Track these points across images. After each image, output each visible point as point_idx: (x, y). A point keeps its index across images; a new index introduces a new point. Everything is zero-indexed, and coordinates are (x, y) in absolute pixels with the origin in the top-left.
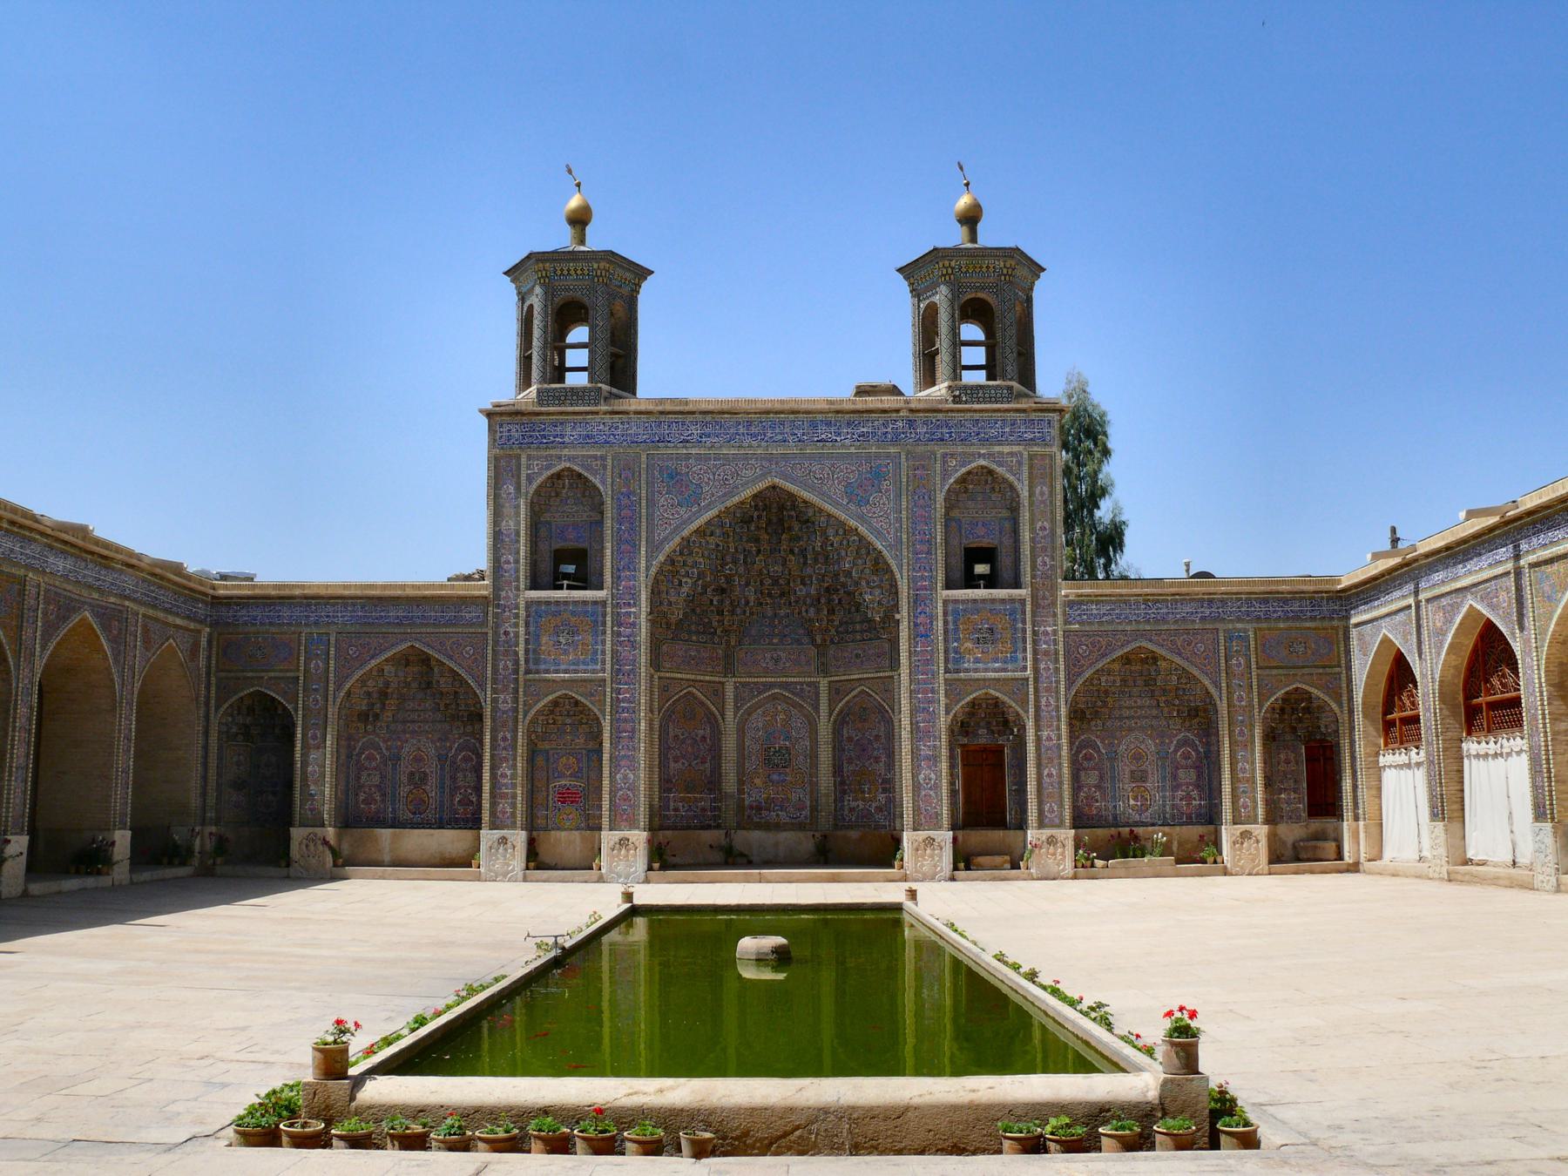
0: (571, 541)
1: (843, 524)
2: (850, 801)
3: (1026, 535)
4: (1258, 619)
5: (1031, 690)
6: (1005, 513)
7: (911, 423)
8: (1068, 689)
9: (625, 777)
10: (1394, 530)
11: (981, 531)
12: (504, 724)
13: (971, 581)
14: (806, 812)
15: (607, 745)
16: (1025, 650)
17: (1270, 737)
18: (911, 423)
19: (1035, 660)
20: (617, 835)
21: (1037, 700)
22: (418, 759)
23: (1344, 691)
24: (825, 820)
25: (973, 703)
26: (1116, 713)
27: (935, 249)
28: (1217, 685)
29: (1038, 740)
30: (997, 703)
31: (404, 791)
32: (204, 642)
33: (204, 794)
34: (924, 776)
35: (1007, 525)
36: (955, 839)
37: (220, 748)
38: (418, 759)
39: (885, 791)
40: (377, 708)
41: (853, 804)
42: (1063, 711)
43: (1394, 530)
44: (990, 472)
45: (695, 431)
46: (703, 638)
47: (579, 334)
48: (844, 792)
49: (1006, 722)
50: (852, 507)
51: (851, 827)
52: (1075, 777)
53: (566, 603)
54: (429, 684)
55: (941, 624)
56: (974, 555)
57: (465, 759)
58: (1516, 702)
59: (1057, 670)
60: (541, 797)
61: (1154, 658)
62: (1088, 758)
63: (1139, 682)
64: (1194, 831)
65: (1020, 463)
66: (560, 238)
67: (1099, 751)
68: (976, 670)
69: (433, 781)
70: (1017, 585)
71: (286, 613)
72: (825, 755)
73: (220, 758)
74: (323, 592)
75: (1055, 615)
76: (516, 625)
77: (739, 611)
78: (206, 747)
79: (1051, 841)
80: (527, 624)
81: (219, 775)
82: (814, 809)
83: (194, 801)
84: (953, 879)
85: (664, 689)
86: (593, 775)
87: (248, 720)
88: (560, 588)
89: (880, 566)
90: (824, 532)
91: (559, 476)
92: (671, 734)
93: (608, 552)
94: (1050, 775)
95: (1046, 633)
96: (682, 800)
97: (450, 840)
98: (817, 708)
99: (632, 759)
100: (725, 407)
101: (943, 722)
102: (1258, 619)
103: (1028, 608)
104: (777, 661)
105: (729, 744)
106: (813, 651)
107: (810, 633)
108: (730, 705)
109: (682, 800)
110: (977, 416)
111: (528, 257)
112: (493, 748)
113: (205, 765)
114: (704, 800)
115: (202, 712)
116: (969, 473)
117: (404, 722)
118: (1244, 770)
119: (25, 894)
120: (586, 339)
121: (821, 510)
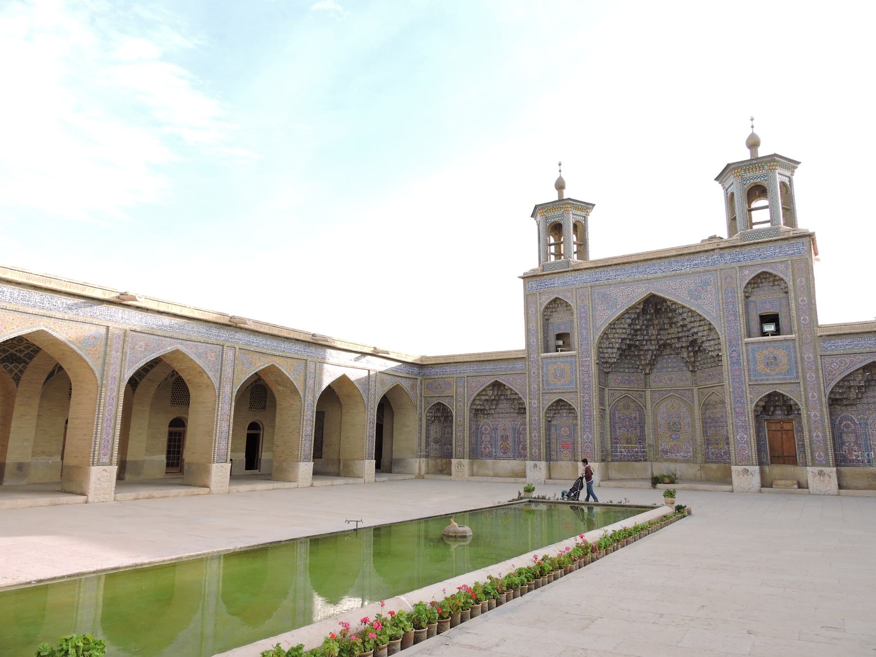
1: (691, 311)
3: (793, 305)
5: (802, 389)
6: (783, 295)
9: (588, 437)
12: (534, 413)
16: (797, 367)
18: (721, 255)
22: (505, 430)
25: (769, 395)
27: (728, 165)
29: (809, 416)
30: (783, 396)
31: (499, 443)
32: (419, 383)
34: (742, 434)
37: (427, 426)
38: (505, 430)
40: (487, 408)
41: (713, 450)
42: (825, 400)
45: (612, 274)
46: (632, 370)
48: (709, 444)
49: (791, 406)
50: (692, 301)
51: (712, 462)
53: (559, 357)
55: (745, 356)
59: (818, 377)
60: (553, 446)
62: (848, 426)
65: (787, 268)
66: (554, 196)
67: (854, 423)
68: (767, 380)
72: (698, 425)
73: (428, 431)
76: (538, 369)
77: (648, 357)
79: (821, 473)
81: (427, 437)
82: (695, 452)
83: (416, 446)
84: (760, 491)
87: (439, 414)
92: (617, 416)
93: (576, 334)
94: (817, 436)
95: (809, 358)
96: (624, 448)
98: (693, 402)
100: (625, 261)
101: (750, 407)
103: (797, 345)
105: (649, 420)
106: (689, 374)
109: (624, 448)
110: (758, 246)
111: (536, 208)
114: (637, 448)
116: (758, 276)
117: (499, 413)
119: (312, 486)
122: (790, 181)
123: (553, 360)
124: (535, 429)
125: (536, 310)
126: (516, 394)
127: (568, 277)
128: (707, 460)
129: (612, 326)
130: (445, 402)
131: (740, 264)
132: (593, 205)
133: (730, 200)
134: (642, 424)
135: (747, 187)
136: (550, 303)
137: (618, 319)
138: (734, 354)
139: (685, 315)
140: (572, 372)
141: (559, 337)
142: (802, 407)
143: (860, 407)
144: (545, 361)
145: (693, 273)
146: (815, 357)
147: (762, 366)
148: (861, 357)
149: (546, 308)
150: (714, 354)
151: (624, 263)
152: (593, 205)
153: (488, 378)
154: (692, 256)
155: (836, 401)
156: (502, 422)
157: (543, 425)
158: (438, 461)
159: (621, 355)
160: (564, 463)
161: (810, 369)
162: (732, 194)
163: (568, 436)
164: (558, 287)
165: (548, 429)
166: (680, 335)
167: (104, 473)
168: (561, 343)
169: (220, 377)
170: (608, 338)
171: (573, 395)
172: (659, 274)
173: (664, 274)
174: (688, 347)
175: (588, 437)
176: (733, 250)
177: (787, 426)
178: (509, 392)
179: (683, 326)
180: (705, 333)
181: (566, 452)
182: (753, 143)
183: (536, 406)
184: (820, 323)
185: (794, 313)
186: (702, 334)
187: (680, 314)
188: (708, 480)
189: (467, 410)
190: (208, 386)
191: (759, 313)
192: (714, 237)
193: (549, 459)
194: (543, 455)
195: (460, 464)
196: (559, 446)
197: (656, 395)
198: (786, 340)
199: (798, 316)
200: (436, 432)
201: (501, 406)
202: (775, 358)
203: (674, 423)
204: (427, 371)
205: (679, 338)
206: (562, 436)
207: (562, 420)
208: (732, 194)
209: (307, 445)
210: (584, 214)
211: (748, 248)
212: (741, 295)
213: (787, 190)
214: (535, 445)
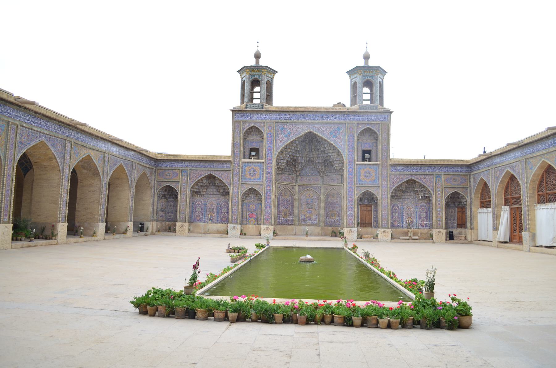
0: (254, 146)
1: (329, 143)
2: (329, 219)
3: (380, 147)
6: (375, 141)
7: (349, 115)
8: (390, 190)
9: (268, 211)
10: (484, 148)
11: (367, 145)
12: (235, 195)
13: (364, 159)
14: (317, 222)
15: (263, 202)
17: (447, 205)
18: (349, 115)
19: (382, 182)
20: (265, 226)
21: (382, 193)
24: (322, 223)
25: (364, 193)
26: (404, 197)
28: (432, 189)
29: (382, 203)
31: (207, 213)
32: (154, 171)
33: (153, 213)
35: (375, 145)
36: (358, 231)
37: (158, 201)
39: (339, 216)
40: (201, 190)
42: (389, 196)
43: (484, 148)
44: (370, 129)
45: (289, 116)
46: (290, 173)
47: (257, 89)
49: (373, 198)
50: (332, 138)
52: (392, 214)
54: (215, 184)
56: (365, 152)
57: (225, 205)
58: (520, 198)
59: (387, 185)
60: (244, 216)
61: (415, 182)
62: (395, 209)
63: (411, 189)
64: (426, 230)
66: (252, 62)
69: (215, 211)
70: (377, 161)
71: (176, 164)
72: (322, 206)
73: (157, 203)
74: (186, 159)
75: (388, 169)
76: (239, 169)
78: (154, 200)
79: (384, 232)
80: (242, 168)
81: (157, 208)
83: (150, 214)
85: (279, 187)
86: (259, 210)
87: (166, 193)
88: (251, 159)
89: (339, 154)
90: (324, 145)
91: (251, 128)
93: (265, 149)
95: (384, 174)
97: (220, 226)
99: (270, 206)
101: (356, 198)
102: (445, 172)
104: (310, 180)
105: (296, 202)
106: (320, 178)
107: (319, 172)
108: (297, 192)
111: (244, 67)
112: (232, 202)
113: (153, 205)
115: (153, 190)
116: (364, 129)
117: (208, 194)
119: (104, 239)
120: (259, 91)
121: (323, 139)
122: (382, 80)
123: (249, 164)
124: (235, 205)
125: (240, 131)
126: (223, 183)
127: (262, 115)
128: (326, 224)
129: (286, 148)
130: (173, 185)
131: (357, 122)
132: (277, 72)
133: (354, 86)
134: (292, 204)
135: (364, 80)
136: (249, 129)
137: (289, 144)
138: (350, 170)
139: (326, 146)
140: (260, 172)
141: (252, 150)
142: (379, 199)
143: (401, 200)
144: (244, 164)
145: (334, 123)
146: (387, 174)
147: (363, 177)
148: (406, 176)
149: (246, 131)
150: (338, 168)
151: (296, 111)
152: (277, 72)
153: (205, 172)
154: (334, 114)
155: (394, 197)
156: (212, 200)
157: (240, 203)
158: (164, 223)
159: (287, 165)
160: (251, 226)
161: (384, 180)
162: (355, 83)
163: (254, 210)
164: (255, 120)
165: (242, 206)
166: (319, 156)
167: (6, 229)
168: (254, 153)
169: (64, 162)
170: (282, 154)
171: (260, 186)
172: (315, 121)
173: (318, 121)
174: (322, 163)
175: (268, 211)
176: (355, 114)
177: (369, 208)
178: (217, 182)
179: (322, 151)
180: (335, 156)
181: (252, 219)
182: (367, 57)
183: (236, 191)
184: (391, 157)
185: (380, 151)
186: (334, 156)
187: (324, 145)
188: (326, 235)
189: (188, 191)
190: (53, 168)
191: (363, 149)
192: (339, 103)
193: (242, 224)
194: (239, 221)
195: (182, 226)
196: (248, 215)
197: (301, 188)
198: (375, 165)
199: (382, 153)
200: (163, 205)
201: (210, 190)
202: (369, 173)
203: (310, 204)
204: (160, 164)
205: (318, 158)
206: (250, 210)
207: (252, 201)
208: (355, 83)
209: (102, 212)
210: (271, 77)
211: (362, 114)
212: (356, 138)
213: (381, 85)
214: (235, 215)
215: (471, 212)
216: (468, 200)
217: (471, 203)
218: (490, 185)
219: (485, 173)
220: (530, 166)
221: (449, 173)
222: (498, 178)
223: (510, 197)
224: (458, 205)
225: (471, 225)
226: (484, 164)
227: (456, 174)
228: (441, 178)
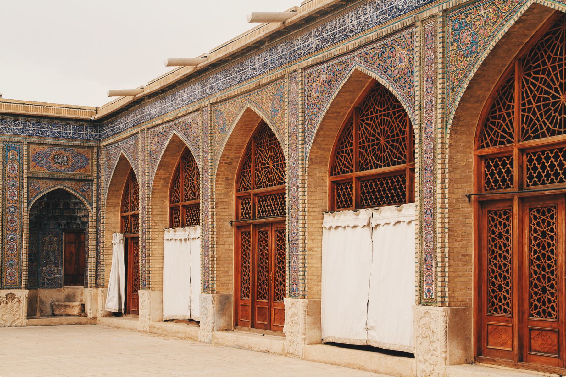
4: (32, 135)
17: (36, 226)
23: (94, 194)
102: (32, 135)
118: (12, 249)
215: (98, 242)
216: (93, 213)
217: (98, 221)
218: (138, 172)
219: (131, 142)
220: (221, 122)
221: (43, 140)
222: (153, 154)
223: (181, 204)
224: (67, 224)
225: (97, 276)
226: (129, 119)
227: (62, 142)
228: (19, 151)
